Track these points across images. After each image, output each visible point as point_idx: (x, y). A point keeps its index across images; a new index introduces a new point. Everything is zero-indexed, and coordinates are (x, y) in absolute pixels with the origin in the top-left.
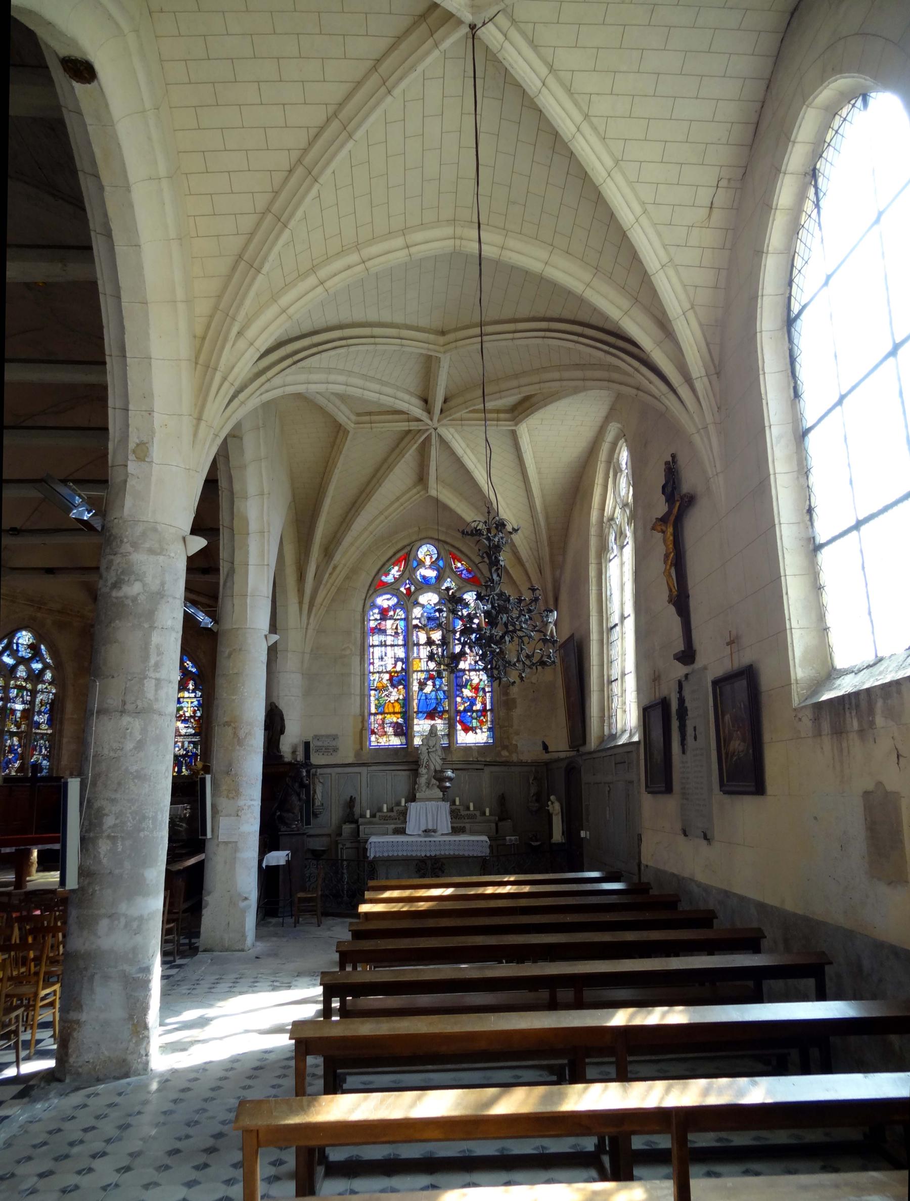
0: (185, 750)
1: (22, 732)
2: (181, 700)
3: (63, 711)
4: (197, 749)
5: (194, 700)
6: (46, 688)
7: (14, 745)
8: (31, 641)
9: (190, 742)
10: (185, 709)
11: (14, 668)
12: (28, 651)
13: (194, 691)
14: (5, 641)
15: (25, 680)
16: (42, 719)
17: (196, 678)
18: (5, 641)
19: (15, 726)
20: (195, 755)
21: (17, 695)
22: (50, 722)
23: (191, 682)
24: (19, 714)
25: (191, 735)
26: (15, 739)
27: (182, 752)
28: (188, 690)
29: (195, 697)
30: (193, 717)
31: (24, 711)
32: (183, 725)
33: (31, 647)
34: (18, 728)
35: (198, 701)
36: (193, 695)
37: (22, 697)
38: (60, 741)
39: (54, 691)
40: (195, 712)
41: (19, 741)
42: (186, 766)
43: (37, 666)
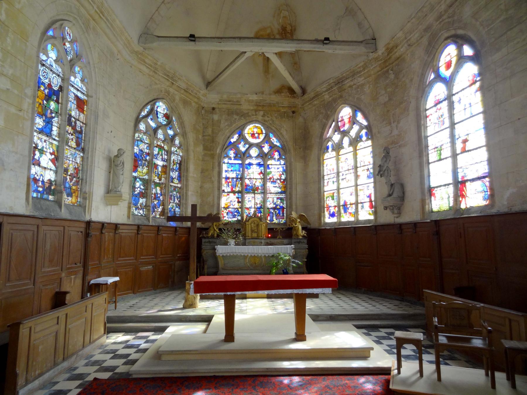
0: (275, 204)
1: (162, 183)
2: (270, 166)
3: (187, 170)
4: (283, 204)
5: (280, 166)
6: (176, 151)
7: (157, 194)
8: (166, 111)
9: (278, 198)
10: (273, 173)
11: (155, 131)
12: (164, 119)
13: (279, 160)
14: (149, 107)
15: (163, 142)
16: (174, 175)
17: (281, 150)
18: (149, 107)
19: (158, 178)
20: (283, 208)
21: (158, 154)
22: (180, 178)
23: (276, 154)
24: (160, 169)
25: (278, 193)
26: (158, 188)
27: (272, 206)
28: (275, 159)
29: (280, 164)
30: (280, 179)
31: (163, 166)
32: (273, 185)
33: (166, 116)
34: (160, 180)
35: (283, 167)
36: (278, 163)
37: (162, 155)
38: (186, 193)
39: (181, 154)
40: (280, 175)
41: (161, 190)
42: (276, 216)
43: (171, 132)
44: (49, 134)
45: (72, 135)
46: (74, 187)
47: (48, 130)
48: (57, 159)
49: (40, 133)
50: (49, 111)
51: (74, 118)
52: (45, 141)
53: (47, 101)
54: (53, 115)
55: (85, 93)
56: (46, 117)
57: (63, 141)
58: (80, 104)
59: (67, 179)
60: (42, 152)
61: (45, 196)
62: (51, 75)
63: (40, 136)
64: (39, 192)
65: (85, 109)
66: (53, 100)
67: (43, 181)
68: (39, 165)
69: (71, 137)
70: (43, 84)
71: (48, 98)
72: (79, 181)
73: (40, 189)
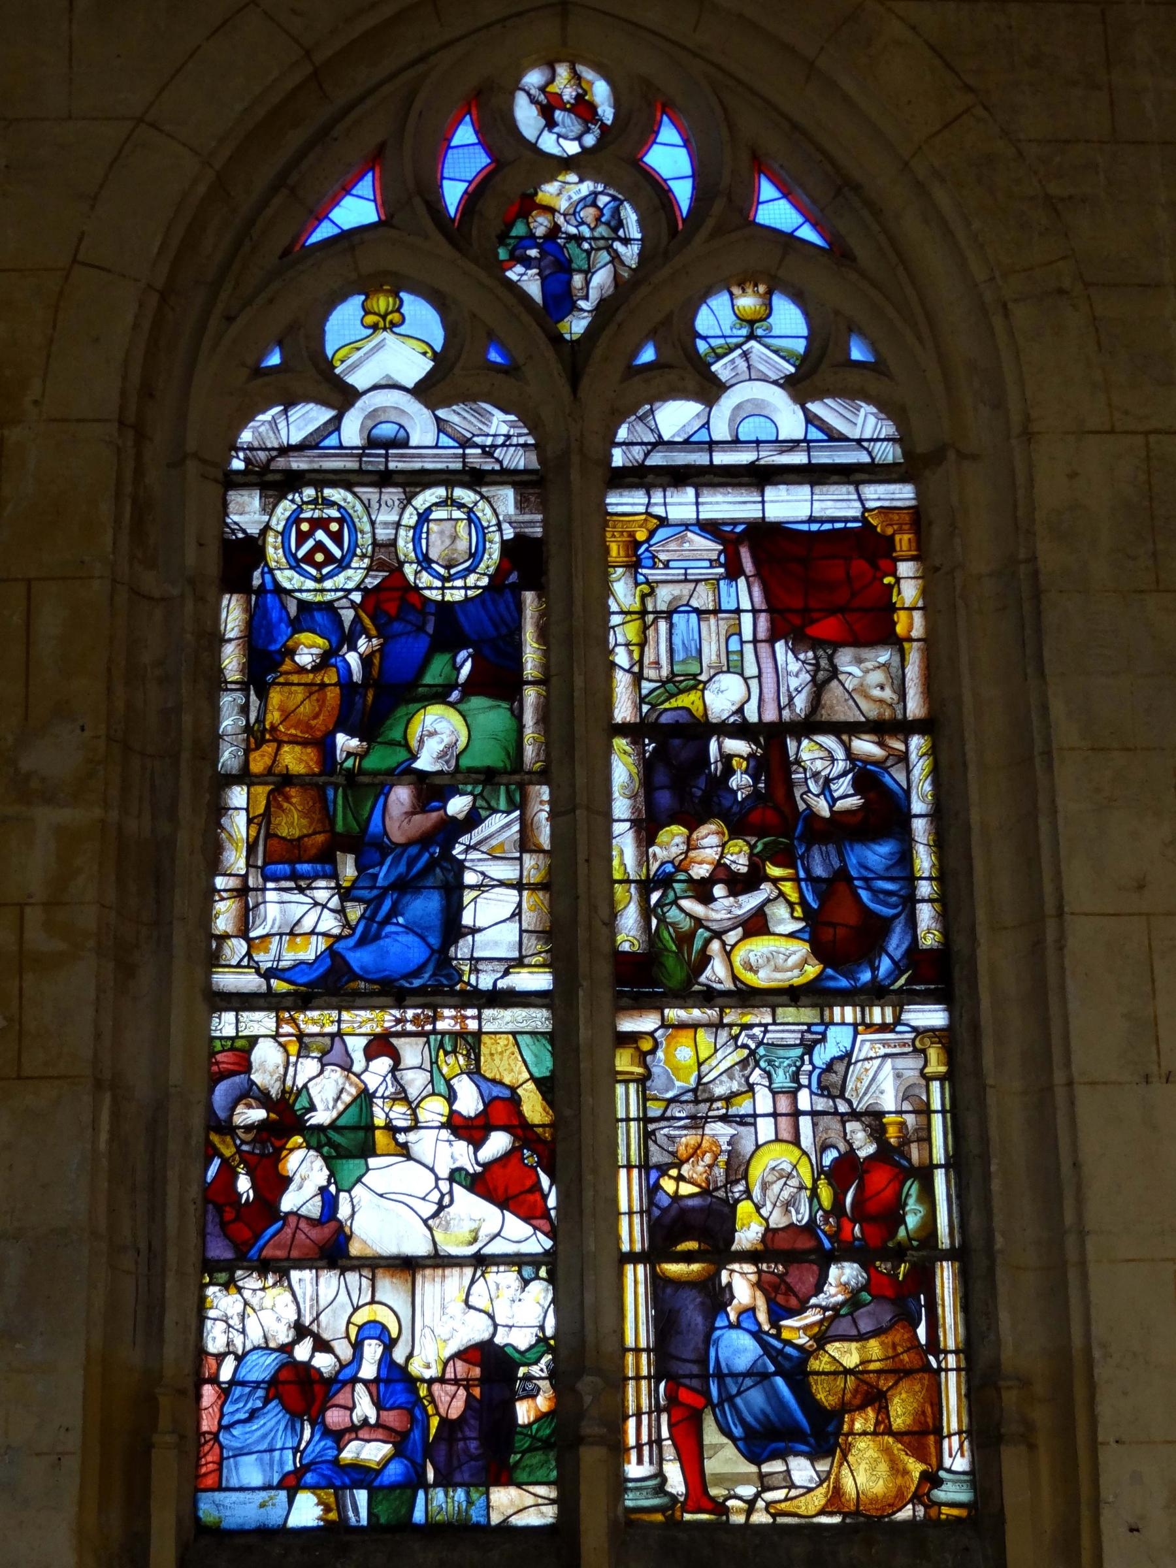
44: (436, 981)
45: (740, 885)
46: (849, 1355)
47: (402, 949)
48: (545, 1158)
49: (304, 1000)
50: (402, 795)
51: (742, 730)
52: (380, 1045)
53: (369, 731)
54: (458, 806)
55: (887, 453)
56: (369, 847)
57: (611, 978)
58: (813, 587)
59: (716, 1297)
60: (353, 1142)
61: (436, 1503)
62: (385, 516)
63: (314, 1021)
64: (361, 1475)
65: (909, 592)
66: (439, 695)
67: (395, 1380)
68: (332, 1249)
69: (725, 907)
70: (312, 614)
71: (379, 703)
72: (924, 1280)
73: (373, 1452)
